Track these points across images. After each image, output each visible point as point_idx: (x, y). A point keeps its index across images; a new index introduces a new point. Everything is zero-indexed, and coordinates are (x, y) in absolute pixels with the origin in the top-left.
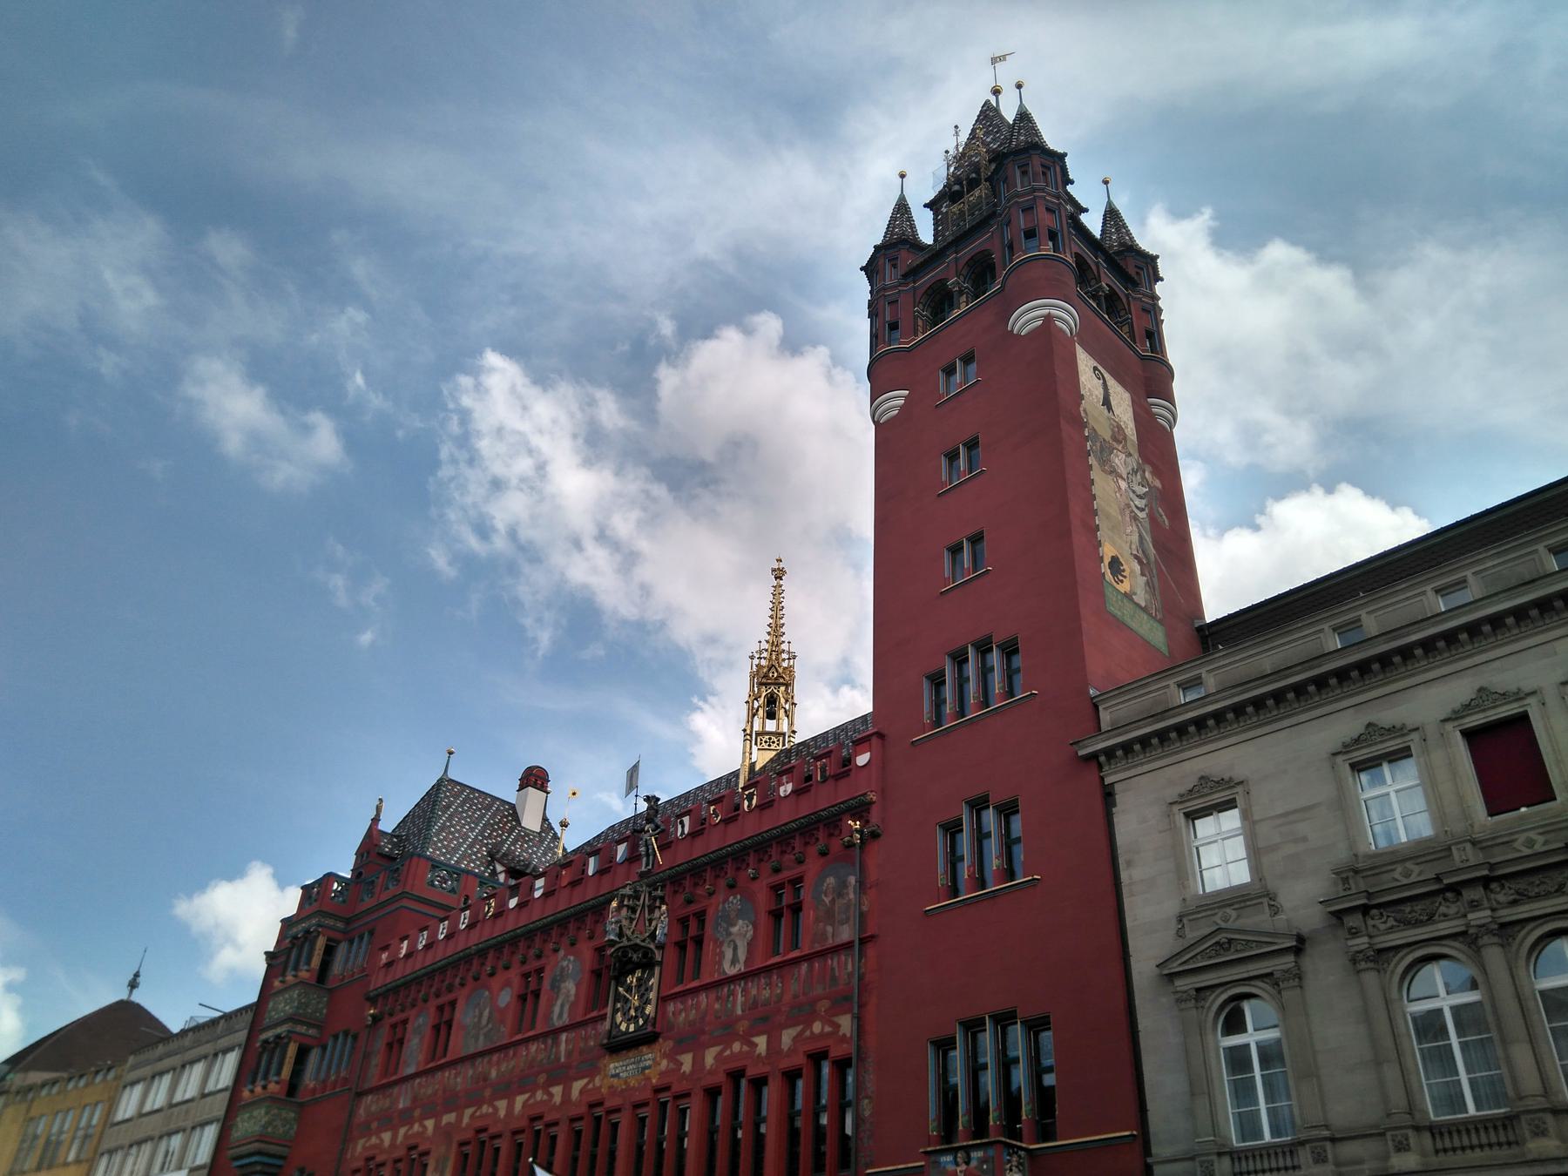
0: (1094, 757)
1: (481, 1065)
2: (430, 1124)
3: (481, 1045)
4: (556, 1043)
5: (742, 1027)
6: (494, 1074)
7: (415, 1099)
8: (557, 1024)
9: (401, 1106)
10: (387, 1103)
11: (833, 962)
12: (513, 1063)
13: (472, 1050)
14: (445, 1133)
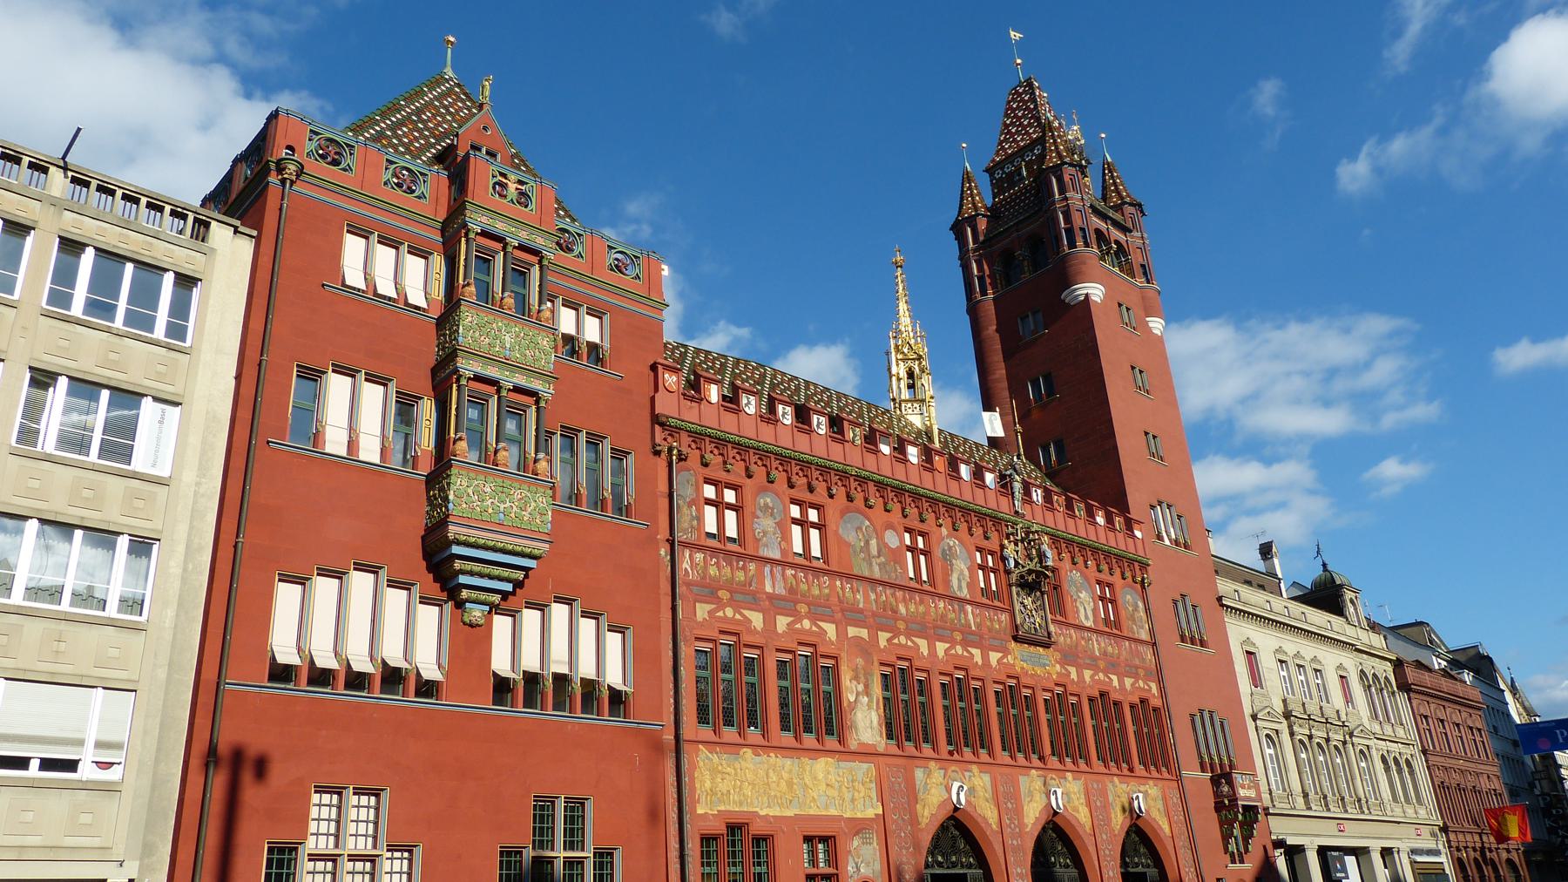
0: (1223, 605)
1: (886, 595)
2: (830, 629)
3: (877, 574)
4: (966, 614)
5: (1102, 664)
6: (903, 610)
7: (792, 590)
8: (959, 594)
9: (769, 589)
10: (740, 576)
11: (1141, 648)
12: (922, 609)
13: (866, 574)
14: (865, 649)
